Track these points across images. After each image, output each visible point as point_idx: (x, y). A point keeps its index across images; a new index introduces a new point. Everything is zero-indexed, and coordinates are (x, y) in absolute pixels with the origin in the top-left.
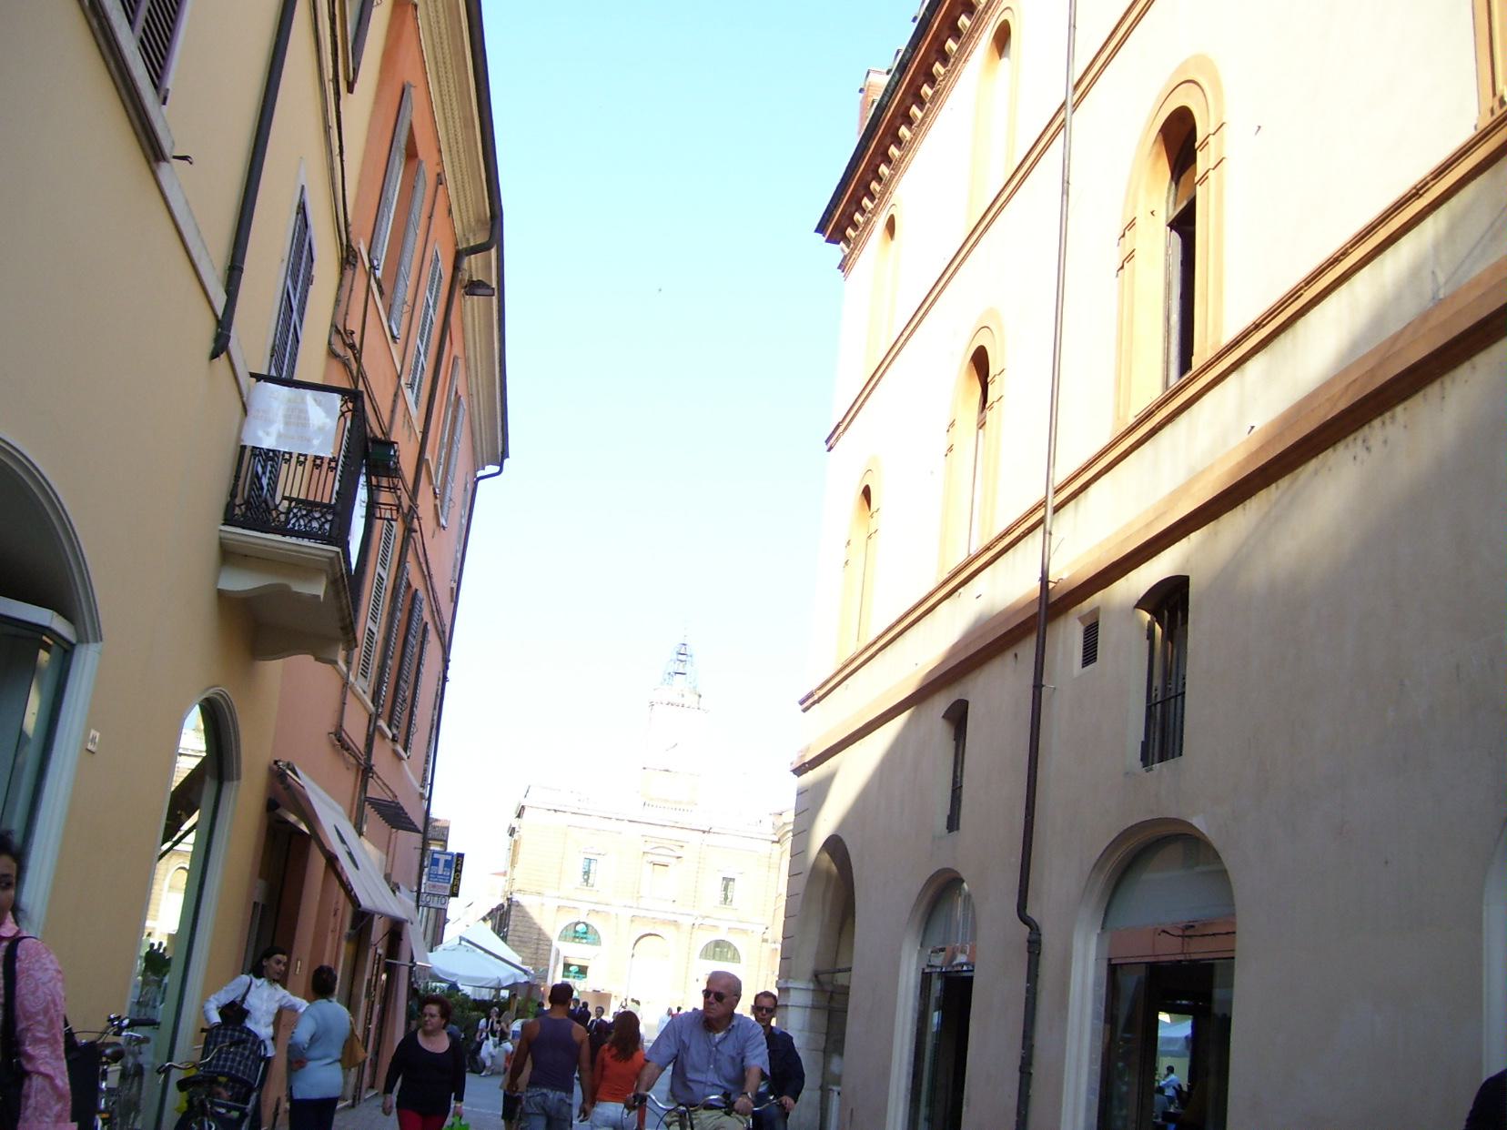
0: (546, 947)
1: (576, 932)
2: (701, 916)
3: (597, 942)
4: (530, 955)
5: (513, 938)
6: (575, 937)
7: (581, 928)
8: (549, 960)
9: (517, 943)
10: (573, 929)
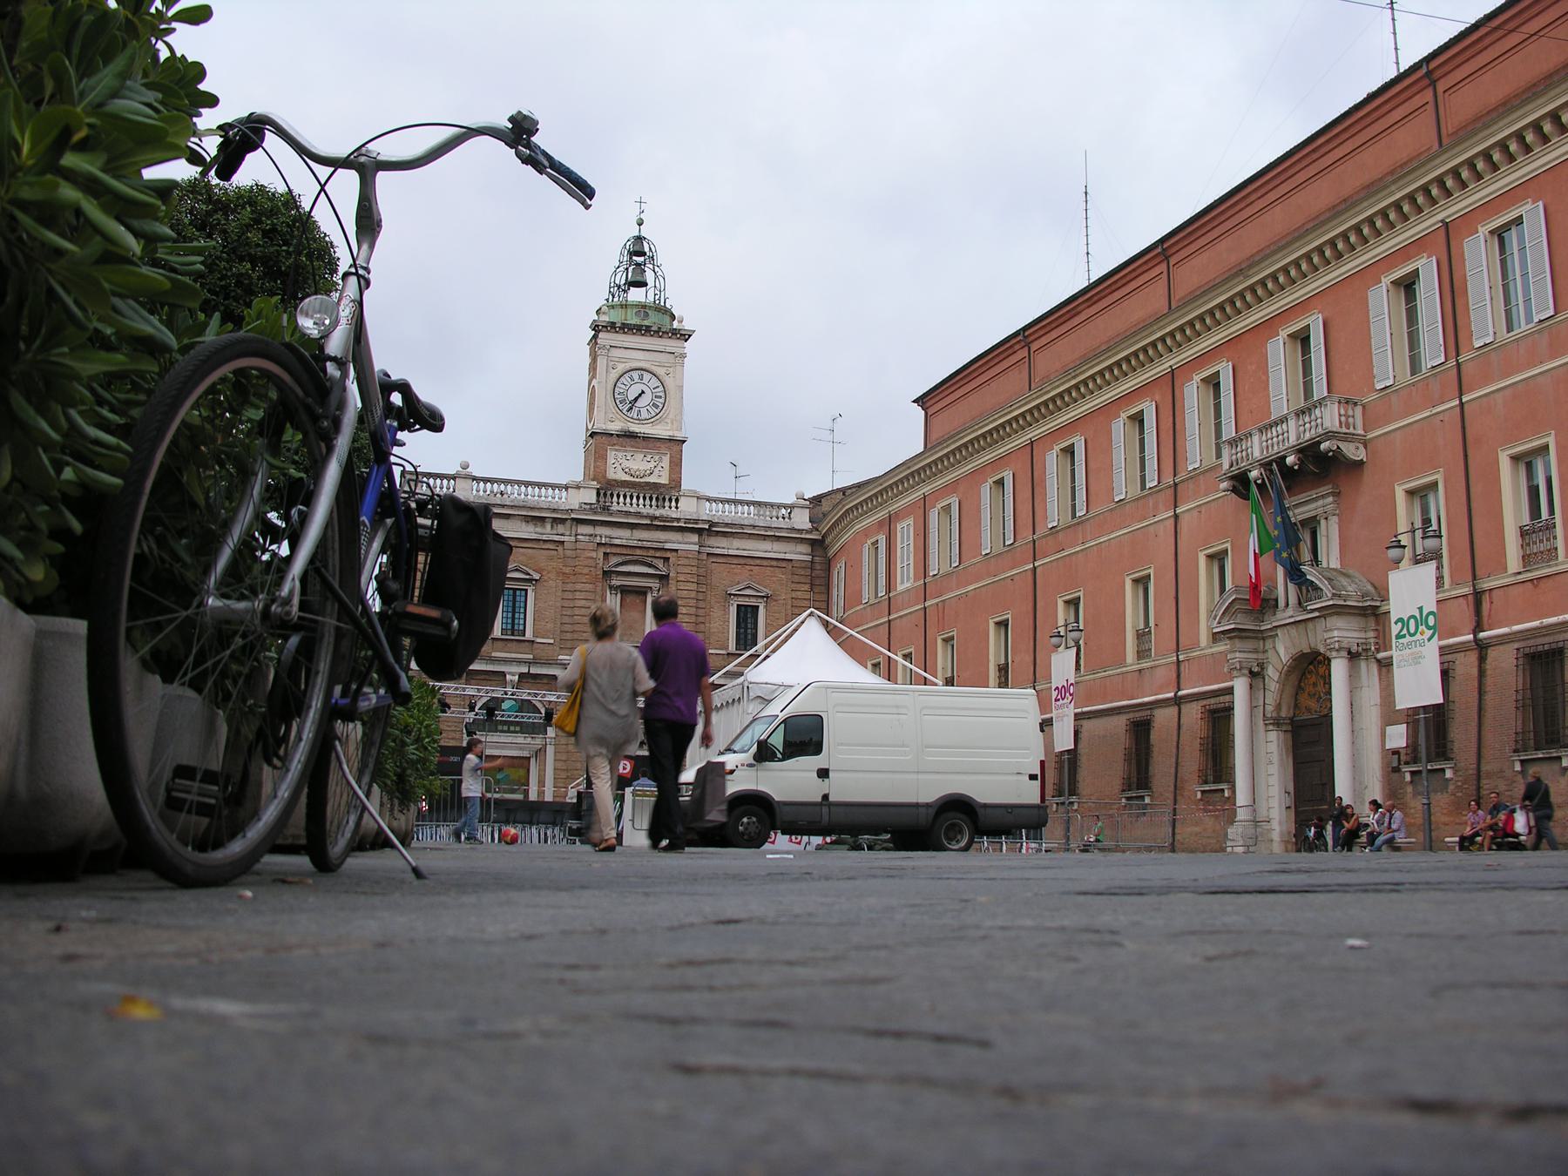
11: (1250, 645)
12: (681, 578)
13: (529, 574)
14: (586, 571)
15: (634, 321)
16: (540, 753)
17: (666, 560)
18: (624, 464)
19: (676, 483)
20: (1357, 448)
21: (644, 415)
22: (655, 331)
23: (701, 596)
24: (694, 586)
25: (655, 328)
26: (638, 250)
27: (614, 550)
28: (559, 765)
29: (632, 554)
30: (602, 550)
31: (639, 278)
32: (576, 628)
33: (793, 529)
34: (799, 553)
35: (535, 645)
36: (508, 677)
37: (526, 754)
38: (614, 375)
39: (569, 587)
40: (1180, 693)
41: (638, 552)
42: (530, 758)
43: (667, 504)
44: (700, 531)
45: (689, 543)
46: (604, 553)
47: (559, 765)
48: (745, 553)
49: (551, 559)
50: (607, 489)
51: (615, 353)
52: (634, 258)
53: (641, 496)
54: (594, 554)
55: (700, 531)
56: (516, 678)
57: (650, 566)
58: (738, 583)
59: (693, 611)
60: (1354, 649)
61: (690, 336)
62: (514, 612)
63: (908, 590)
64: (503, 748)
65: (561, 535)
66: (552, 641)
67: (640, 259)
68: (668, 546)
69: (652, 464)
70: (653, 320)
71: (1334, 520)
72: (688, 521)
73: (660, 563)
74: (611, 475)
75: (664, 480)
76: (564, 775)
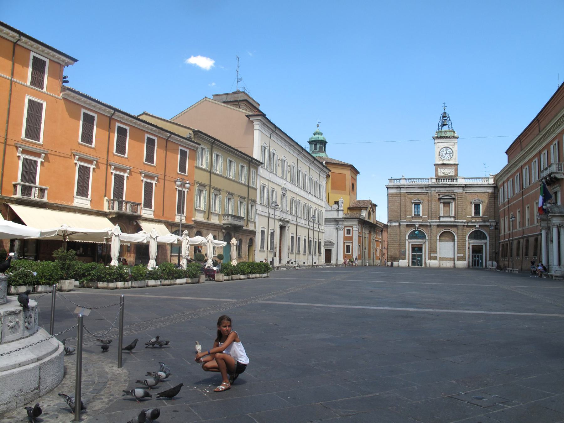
0: (404, 242)
3: (424, 237)
4: (397, 246)
5: (391, 240)
8: (405, 247)
9: (392, 242)
11: (546, 222)
14: (434, 199)
15: (443, 135)
16: (425, 243)
17: (455, 195)
18: (442, 172)
19: (456, 175)
21: (448, 158)
23: (464, 203)
24: (462, 201)
26: (445, 117)
27: (441, 193)
29: (445, 194)
31: (445, 123)
33: (488, 184)
37: (421, 244)
38: (439, 150)
41: (447, 193)
42: (422, 245)
44: (463, 187)
45: (460, 190)
48: (475, 191)
49: (425, 196)
50: (438, 178)
51: (438, 144)
52: (445, 118)
54: (436, 195)
55: (463, 187)
56: (418, 226)
57: (450, 196)
59: (461, 207)
60: (559, 225)
61: (458, 137)
62: (417, 210)
64: (416, 243)
67: (446, 118)
68: (455, 191)
69: (450, 171)
70: (448, 134)
71: (560, 192)
72: (459, 184)
73: (453, 196)
74: (439, 174)
75: (453, 175)
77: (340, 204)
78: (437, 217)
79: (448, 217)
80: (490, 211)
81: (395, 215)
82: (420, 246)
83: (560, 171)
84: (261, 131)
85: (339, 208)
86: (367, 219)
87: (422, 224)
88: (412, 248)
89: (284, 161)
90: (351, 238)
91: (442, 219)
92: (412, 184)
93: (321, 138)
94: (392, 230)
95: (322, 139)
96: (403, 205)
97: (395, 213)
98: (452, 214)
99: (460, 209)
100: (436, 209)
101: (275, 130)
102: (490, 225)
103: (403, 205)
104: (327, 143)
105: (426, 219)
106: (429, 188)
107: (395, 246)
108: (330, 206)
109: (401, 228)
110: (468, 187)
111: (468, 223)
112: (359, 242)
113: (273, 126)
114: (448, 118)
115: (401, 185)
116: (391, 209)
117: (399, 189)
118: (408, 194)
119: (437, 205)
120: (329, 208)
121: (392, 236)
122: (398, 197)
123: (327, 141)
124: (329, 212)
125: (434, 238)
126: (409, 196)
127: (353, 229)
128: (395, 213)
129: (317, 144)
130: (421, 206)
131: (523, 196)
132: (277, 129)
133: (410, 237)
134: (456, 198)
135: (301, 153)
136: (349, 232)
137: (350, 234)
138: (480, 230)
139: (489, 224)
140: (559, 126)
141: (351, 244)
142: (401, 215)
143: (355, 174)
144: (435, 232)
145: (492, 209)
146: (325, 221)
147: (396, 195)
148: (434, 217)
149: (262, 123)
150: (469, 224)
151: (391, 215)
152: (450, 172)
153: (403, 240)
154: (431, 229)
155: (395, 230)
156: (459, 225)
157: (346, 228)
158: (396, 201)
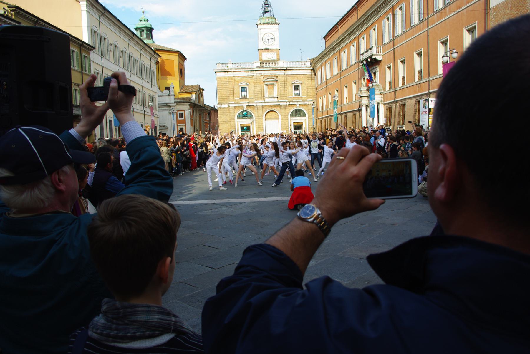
1: (243, 115)
2: (288, 101)
3: (251, 117)
4: (228, 126)
5: (221, 121)
6: (243, 117)
7: (244, 113)
10: (242, 114)
12: (281, 81)
13: (246, 83)
18: (266, 56)
20: (380, 57)
21: (270, 44)
22: (271, 24)
25: (271, 23)
27: (265, 76)
28: (257, 125)
29: (269, 77)
30: (262, 76)
32: (258, 94)
33: (306, 67)
34: (309, 72)
35: (249, 99)
36: (244, 107)
39: (256, 85)
40: (360, 109)
41: (271, 76)
43: (276, 64)
44: (285, 70)
46: (263, 77)
47: (257, 125)
49: (251, 79)
52: (266, 6)
53: (270, 63)
55: (285, 70)
57: (274, 79)
58: (294, 81)
61: (279, 24)
63: (324, 82)
65: (253, 74)
66: (253, 98)
67: (267, 6)
68: (277, 74)
72: (281, 68)
73: (276, 78)
76: (258, 127)
77: (171, 89)
78: (263, 99)
79: (272, 97)
80: (308, 91)
81: (224, 98)
82: (247, 125)
83: (379, 53)
84: (89, 13)
85: (170, 93)
86: (196, 103)
87: (249, 105)
88: (241, 127)
89: (116, 46)
90: (184, 122)
91: (266, 100)
92: (238, 67)
93: (147, 24)
94: (222, 112)
95: (149, 26)
96: (231, 88)
97: (224, 96)
98: (275, 94)
99: (282, 90)
100: (261, 91)
101: (104, 12)
102: (309, 104)
103: (231, 88)
104: (153, 29)
105: (253, 101)
106: (254, 71)
107: (226, 126)
108: (161, 91)
109: (230, 109)
110: (289, 70)
111: (289, 103)
112: (191, 125)
113: (102, 7)
114: (270, 6)
115: (229, 69)
116: (220, 92)
117: (227, 73)
118: (235, 77)
119: (262, 87)
120: (161, 94)
121: (222, 117)
122: (226, 81)
123: (153, 27)
124: (161, 97)
125: (260, 117)
126: (237, 79)
127: (185, 112)
128: (224, 96)
129: (143, 31)
130: (247, 88)
131: (341, 77)
132: (106, 11)
133: (239, 117)
134: (279, 80)
135: (132, 38)
136: (181, 115)
137: (182, 117)
138: (300, 108)
139: (307, 103)
140: (379, 12)
141: (184, 127)
142: (230, 97)
143: (183, 60)
144: (261, 112)
145: (310, 89)
146: (159, 107)
147: (224, 79)
148: (259, 98)
149: (90, 3)
150: (291, 103)
151: (221, 98)
152: (272, 56)
153: (233, 120)
154: (258, 110)
155: (224, 112)
156: (282, 105)
157: (178, 112)
158: (224, 85)
